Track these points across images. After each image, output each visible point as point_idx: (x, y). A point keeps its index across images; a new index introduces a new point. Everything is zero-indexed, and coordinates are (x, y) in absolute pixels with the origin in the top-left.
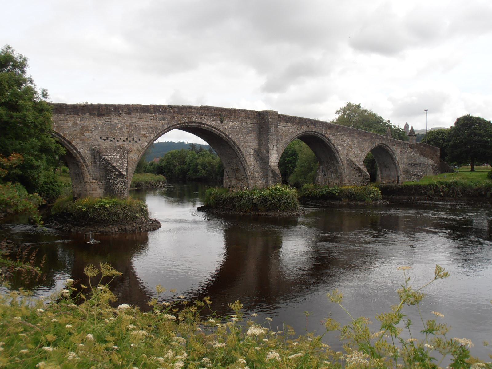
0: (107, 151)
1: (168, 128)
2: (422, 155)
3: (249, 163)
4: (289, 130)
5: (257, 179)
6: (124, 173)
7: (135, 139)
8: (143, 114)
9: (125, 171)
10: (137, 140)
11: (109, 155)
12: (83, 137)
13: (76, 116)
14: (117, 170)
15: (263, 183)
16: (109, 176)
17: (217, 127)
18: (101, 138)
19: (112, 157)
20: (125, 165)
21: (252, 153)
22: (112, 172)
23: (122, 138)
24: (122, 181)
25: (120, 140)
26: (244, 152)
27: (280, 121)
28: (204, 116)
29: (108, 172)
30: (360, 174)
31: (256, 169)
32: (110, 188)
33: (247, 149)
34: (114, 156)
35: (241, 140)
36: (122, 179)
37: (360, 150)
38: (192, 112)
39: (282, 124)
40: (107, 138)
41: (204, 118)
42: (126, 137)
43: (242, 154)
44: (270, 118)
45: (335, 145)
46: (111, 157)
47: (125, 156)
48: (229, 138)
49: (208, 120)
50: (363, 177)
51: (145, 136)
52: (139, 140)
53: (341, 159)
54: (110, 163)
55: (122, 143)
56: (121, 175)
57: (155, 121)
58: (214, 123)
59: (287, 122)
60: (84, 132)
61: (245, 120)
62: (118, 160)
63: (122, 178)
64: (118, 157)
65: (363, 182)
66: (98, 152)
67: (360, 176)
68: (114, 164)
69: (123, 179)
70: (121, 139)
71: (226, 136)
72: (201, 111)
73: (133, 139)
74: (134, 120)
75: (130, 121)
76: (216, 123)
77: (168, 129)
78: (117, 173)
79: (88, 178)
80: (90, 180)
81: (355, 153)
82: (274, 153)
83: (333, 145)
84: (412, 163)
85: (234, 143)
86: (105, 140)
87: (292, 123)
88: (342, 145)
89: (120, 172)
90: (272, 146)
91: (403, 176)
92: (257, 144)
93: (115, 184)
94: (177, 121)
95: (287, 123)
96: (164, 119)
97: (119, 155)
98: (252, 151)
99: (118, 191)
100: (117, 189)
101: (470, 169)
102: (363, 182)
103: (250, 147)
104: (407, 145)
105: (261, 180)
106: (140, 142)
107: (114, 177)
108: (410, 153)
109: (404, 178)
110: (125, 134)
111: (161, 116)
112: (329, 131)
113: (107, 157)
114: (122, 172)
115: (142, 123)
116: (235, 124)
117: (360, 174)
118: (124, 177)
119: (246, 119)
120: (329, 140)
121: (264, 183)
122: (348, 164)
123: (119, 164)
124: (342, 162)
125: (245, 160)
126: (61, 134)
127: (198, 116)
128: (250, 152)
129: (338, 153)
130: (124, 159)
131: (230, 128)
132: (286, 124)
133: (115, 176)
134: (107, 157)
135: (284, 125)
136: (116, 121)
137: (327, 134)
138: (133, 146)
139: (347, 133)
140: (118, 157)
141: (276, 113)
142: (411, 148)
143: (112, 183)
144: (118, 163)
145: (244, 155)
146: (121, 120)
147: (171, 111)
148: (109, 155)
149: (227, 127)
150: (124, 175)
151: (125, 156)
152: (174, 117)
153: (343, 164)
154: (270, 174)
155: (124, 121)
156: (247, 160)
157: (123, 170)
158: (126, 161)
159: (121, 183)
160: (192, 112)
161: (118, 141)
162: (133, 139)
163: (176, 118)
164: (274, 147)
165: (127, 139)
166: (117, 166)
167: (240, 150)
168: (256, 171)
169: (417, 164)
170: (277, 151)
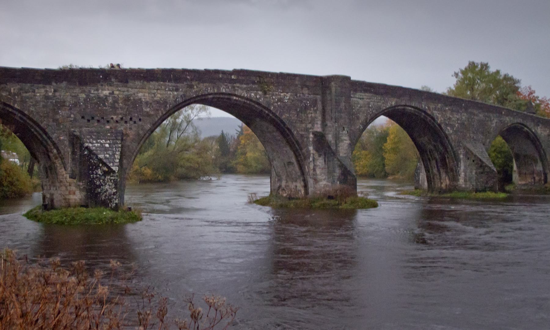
0: (91, 137)
1: (183, 102)
4: (369, 104)
6: (114, 168)
7: (134, 119)
8: (145, 83)
9: (116, 166)
10: (137, 120)
11: (94, 142)
12: (58, 117)
13: (48, 86)
14: (105, 164)
15: (328, 183)
16: (93, 174)
18: (83, 117)
19: (99, 145)
20: (116, 156)
21: (311, 139)
22: (97, 167)
23: (115, 117)
24: (112, 181)
25: (112, 121)
27: (356, 91)
28: (238, 85)
29: (92, 167)
30: (481, 170)
32: (94, 191)
34: (101, 144)
36: (112, 178)
39: (358, 95)
40: (93, 118)
41: (238, 87)
42: (120, 116)
45: (443, 126)
46: (96, 145)
47: (117, 143)
48: (276, 116)
49: (243, 89)
51: (148, 115)
52: (140, 120)
53: (452, 148)
54: (94, 154)
55: (114, 125)
56: (110, 171)
57: (163, 92)
58: (253, 94)
59: (366, 91)
60: (59, 109)
61: (300, 89)
62: (106, 150)
63: (112, 176)
64: (107, 145)
65: (487, 183)
66: (77, 138)
68: (101, 156)
69: (112, 178)
70: (112, 118)
71: (273, 113)
72: (233, 77)
73: (131, 119)
74: (132, 91)
75: (126, 93)
76: (256, 95)
77: (183, 104)
78: (105, 169)
79: (63, 175)
80: (66, 178)
82: (346, 138)
83: (439, 125)
86: (89, 121)
88: (452, 126)
89: (109, 167)
90: (342, 128)
93: (102, 185)
94: (196, 92)
95: (367, 94)
96: (177, 90)
97: (108, 142)
99: (106, 196)
100: (105, 192)
102: (487, 183)
105: (324, 179)
106: (140, 123)
107: (100, 175)
110: (120, 111)
111: (173, 84)
112: (432, 106)
113: (90, 145)
114: (112, 168)
115: (144, 96)
116: (285, 95)
118: (115, 175)
119: (302, 88)
120: (433, 118)
121: (330, 184)
123: (108, 156)
124: (454, 152)
126: (26, 112)
127: (229, 85)
128: (308, 138)
129: (447, 138)
130: (116, 147)
131: (277, 102)
132: (365, 95)
133: (101, 174)
134: (90, 145)
135: (362, 97)
136: (106, 92)
138: (131, 129)
140: (107, 145)
141: (347, 79)
143: (98, 183)
144: (107, 154)
146: (113, 92)
147: (188, 77)
148: (94, 142)
149: (272, 100)
150: (114, 172)
151: (117, 143)
152: (191, 87)
153: (454, 154)
155: (117, 93)
157: (113, 164)
158: (119, 151)
159: (111, 184)
161: (108, 122)
162: (131, 119)
163: (195, 87)
164: (344, 130)
165: (122, 119)
166: (106, 158)
170: (350, 136)
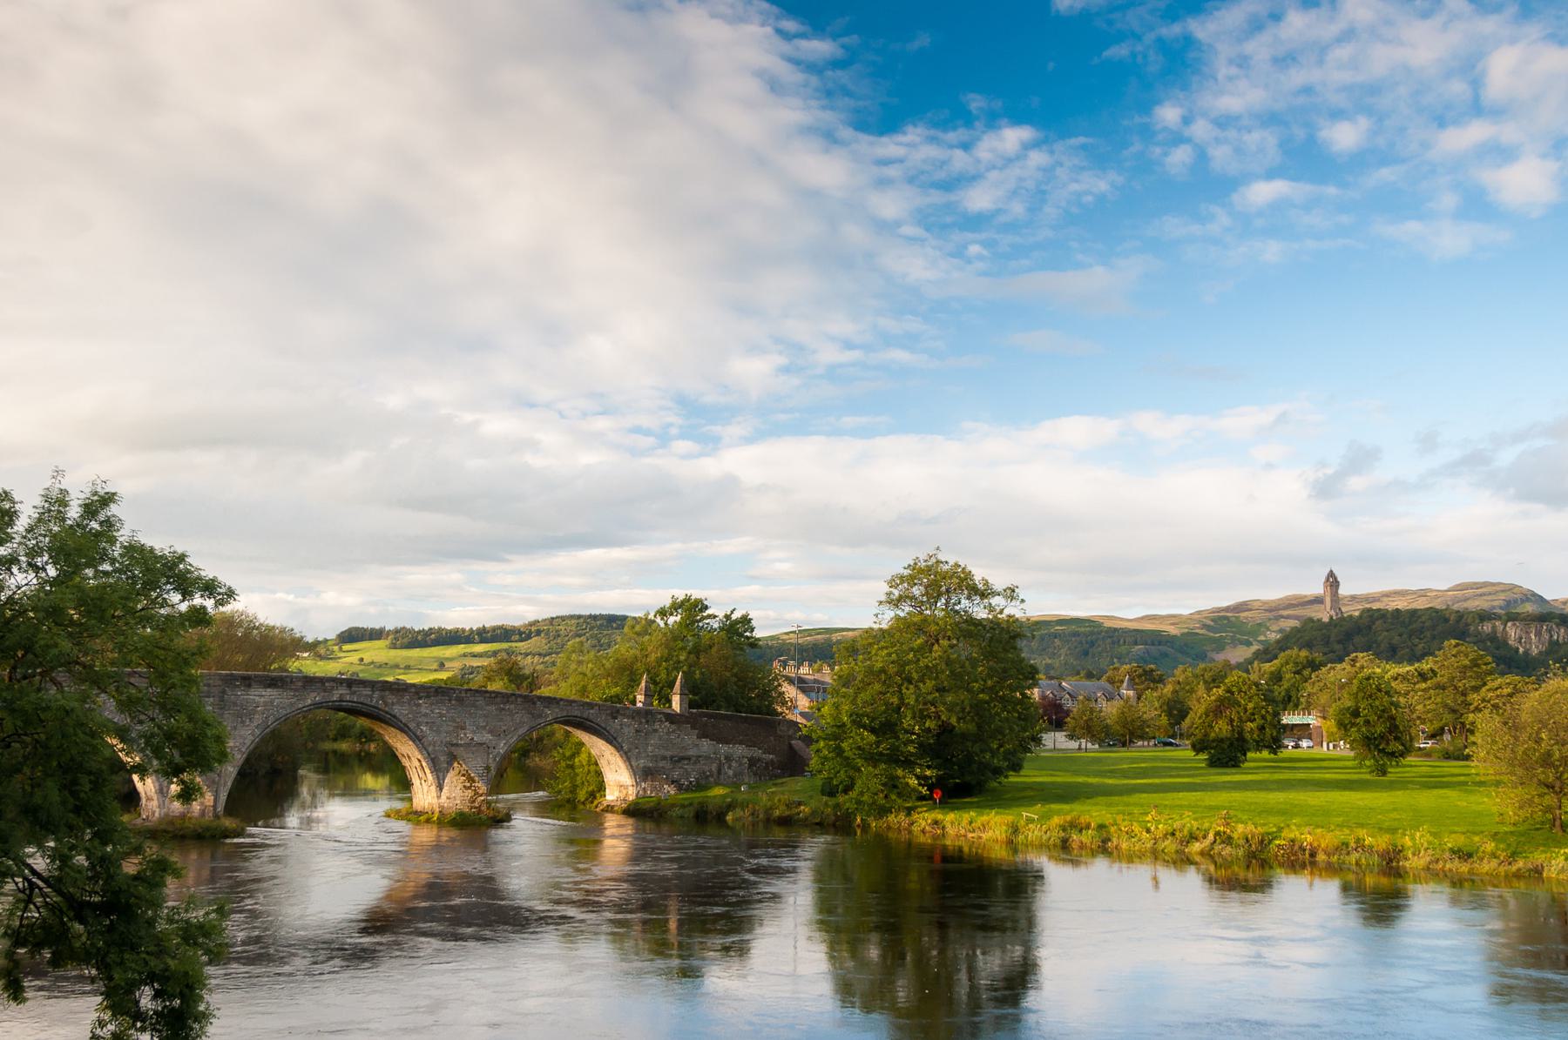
30: (468, 785)
37: (491, 732)
44: (205, 685)
50: (475, 790)
67: (469, 788)
81: (475, 739)
84: (672, 757)
87: (282, 687)
101: (1390, 772)
102: (474, 801)
104: (659, 716)
117: (468, 785)
137: (386, 704)
139: (450, 700)
142: (672, 723)
169: (689, 758)
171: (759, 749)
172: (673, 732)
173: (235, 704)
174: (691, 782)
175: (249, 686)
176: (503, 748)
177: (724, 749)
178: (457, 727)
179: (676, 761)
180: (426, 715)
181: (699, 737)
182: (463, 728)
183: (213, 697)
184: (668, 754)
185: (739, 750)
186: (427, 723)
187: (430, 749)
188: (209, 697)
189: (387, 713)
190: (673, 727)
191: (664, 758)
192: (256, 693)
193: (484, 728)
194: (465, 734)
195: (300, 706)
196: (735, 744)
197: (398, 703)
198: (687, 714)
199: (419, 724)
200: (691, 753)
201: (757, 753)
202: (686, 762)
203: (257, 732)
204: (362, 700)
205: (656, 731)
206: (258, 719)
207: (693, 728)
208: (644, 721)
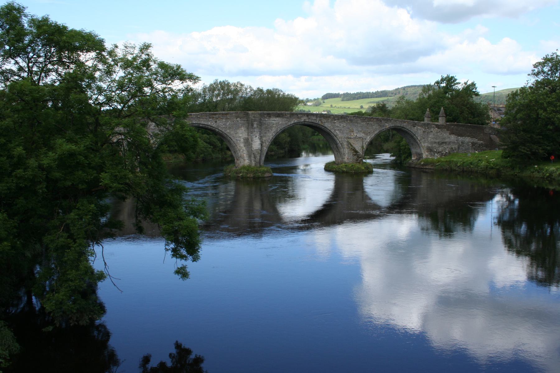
2: (453, 134)
3: (239, 148)
5: (245, 158)
17: (212, 126)
26: (234, 140)
30: (355, 154)
31: (244, 152)
33: (237, 138)
35: (232, 132)
37: (364, 133)
38: (192, 118)
43: (234, 142)
44: (253, 117)
45: (333, 131)
48: (223, 132)
50: (358, 156)
67: (355, 155)
72: (199, 116)
76: (211, 123)
81: (358, 136)
84: (438, 142)
85: (227, 135)
87: (282, 117)
90: (255, 136)
91: (427, 153)
92: (247, 135)
98: (242, 140)
102: (357, 160)
103: (240, 137)
104: (433, 126)
108: (437, 133)
109: (427, 155)
117: (355, 154)
119: (237, 118)
122: (347, 145)
125: (236, 146)
128: (240, 141)
139: (347, 121)
142: (438, 128)
145: (235, 142)
153: (341, 145)
154: (253, 156)
156: (238, 146)
160: (192, 118)
167: (232, 140)
168: (244, 153)
169: (446, 143)
171: (476, 139)
172: (439, 132)
173: (265, 124)
174: (446, 152)
175: (270, 117)
176: (369, 139)
177: (461, 139)
178: (350, 131)
179: (440, 144)
180: (338, 127)
181: (450, 134)
182: (353, 132)
183: (257, 121)
184: (437, 141)
185: (467, 139)
186: (338, 130)
187: (340, 140)
188: (255, 121)
189: (323, 126)
190: (439, 130)
191: (435, 143)
192: (273, 120)
193: (361, 131)
194: (354, 134)
195: (289, 124)
196: (466, 136)
197: (326, 122)
198: (445, 125)
199: (335, 130)
200: (447, 140)
201: (475, 140)
202: (444, 144)
203: (274, 134)
204: (313, 121)
205: (431, 132)
206: (274, 130)
207: (447, 130)
208: (427, 128)
